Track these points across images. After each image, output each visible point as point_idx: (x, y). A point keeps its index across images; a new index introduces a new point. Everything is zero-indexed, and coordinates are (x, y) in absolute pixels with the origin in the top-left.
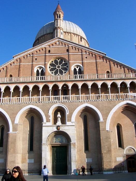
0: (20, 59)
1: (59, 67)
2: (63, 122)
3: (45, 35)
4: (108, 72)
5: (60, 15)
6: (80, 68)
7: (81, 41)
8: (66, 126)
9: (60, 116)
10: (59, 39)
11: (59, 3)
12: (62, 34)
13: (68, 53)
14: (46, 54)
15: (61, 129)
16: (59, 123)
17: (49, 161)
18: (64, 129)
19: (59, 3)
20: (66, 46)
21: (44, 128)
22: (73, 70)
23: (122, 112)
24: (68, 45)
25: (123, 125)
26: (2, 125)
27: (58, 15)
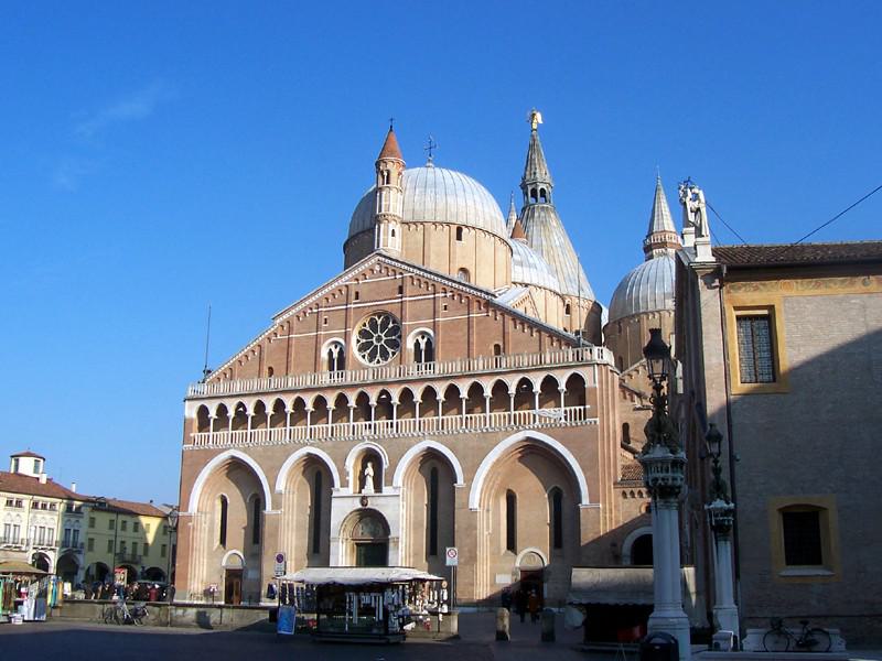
0: (288, 322)
1: (379, 339)
2: (378, 488)
3: (358, 234)
4: (497, 347)
5: (388, 172)
7: (459, 237)
8: (382, 499)
9: (372, 474)
10: (380, 258)
12: (393, 235)
20: (398, 276)
21: (335, 503)
22: (413, 348)
23: (520, 459)
24: (401, 274)
26: (255, 495)
27: (385, 174)
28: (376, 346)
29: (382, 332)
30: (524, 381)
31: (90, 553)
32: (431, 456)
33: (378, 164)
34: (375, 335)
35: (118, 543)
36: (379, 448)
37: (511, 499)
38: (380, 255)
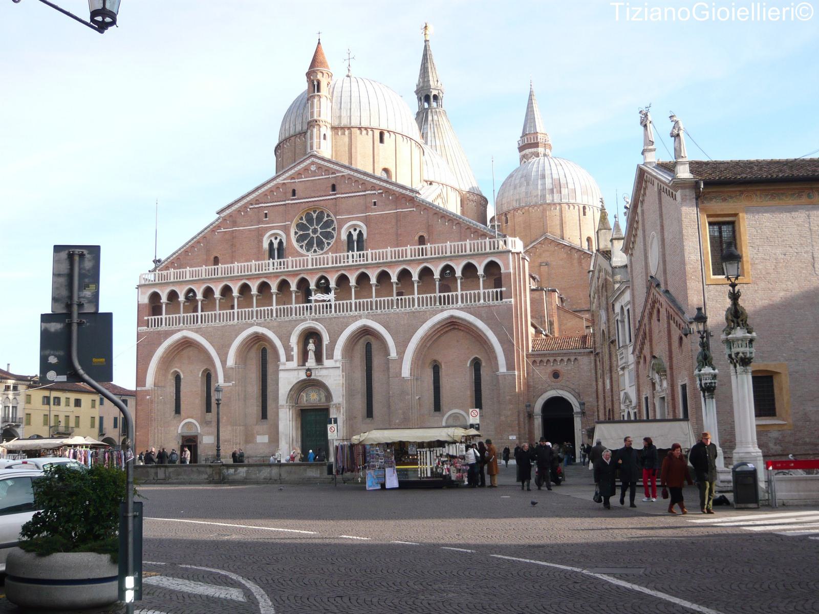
1: (315, 231)
2: (319, 359)
6: (360, 231)
7: (382, 141)
11: (319, 40)
12: (325, 138)
13: (335, 194)
14: (287, 202)
15: (313, 375)
16: (311, 362)
17: (293, 440)
18: (320, 376)
19: (319, 40)
21: (282, 375)
25: (445, 363)
26: (206, 370)
27: (316, 83)
28: (313, 237)
29: (317, 225)
30: (448, 267)
31: (28, 427)
32: (366, 331)
33: (308, 75)
34: (312, 228)
35: (52, 418)
36: (320, 327)
37: (436, 369)
38: (315, 156)
